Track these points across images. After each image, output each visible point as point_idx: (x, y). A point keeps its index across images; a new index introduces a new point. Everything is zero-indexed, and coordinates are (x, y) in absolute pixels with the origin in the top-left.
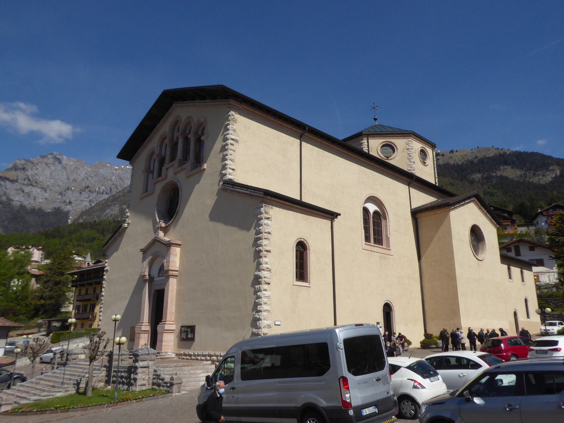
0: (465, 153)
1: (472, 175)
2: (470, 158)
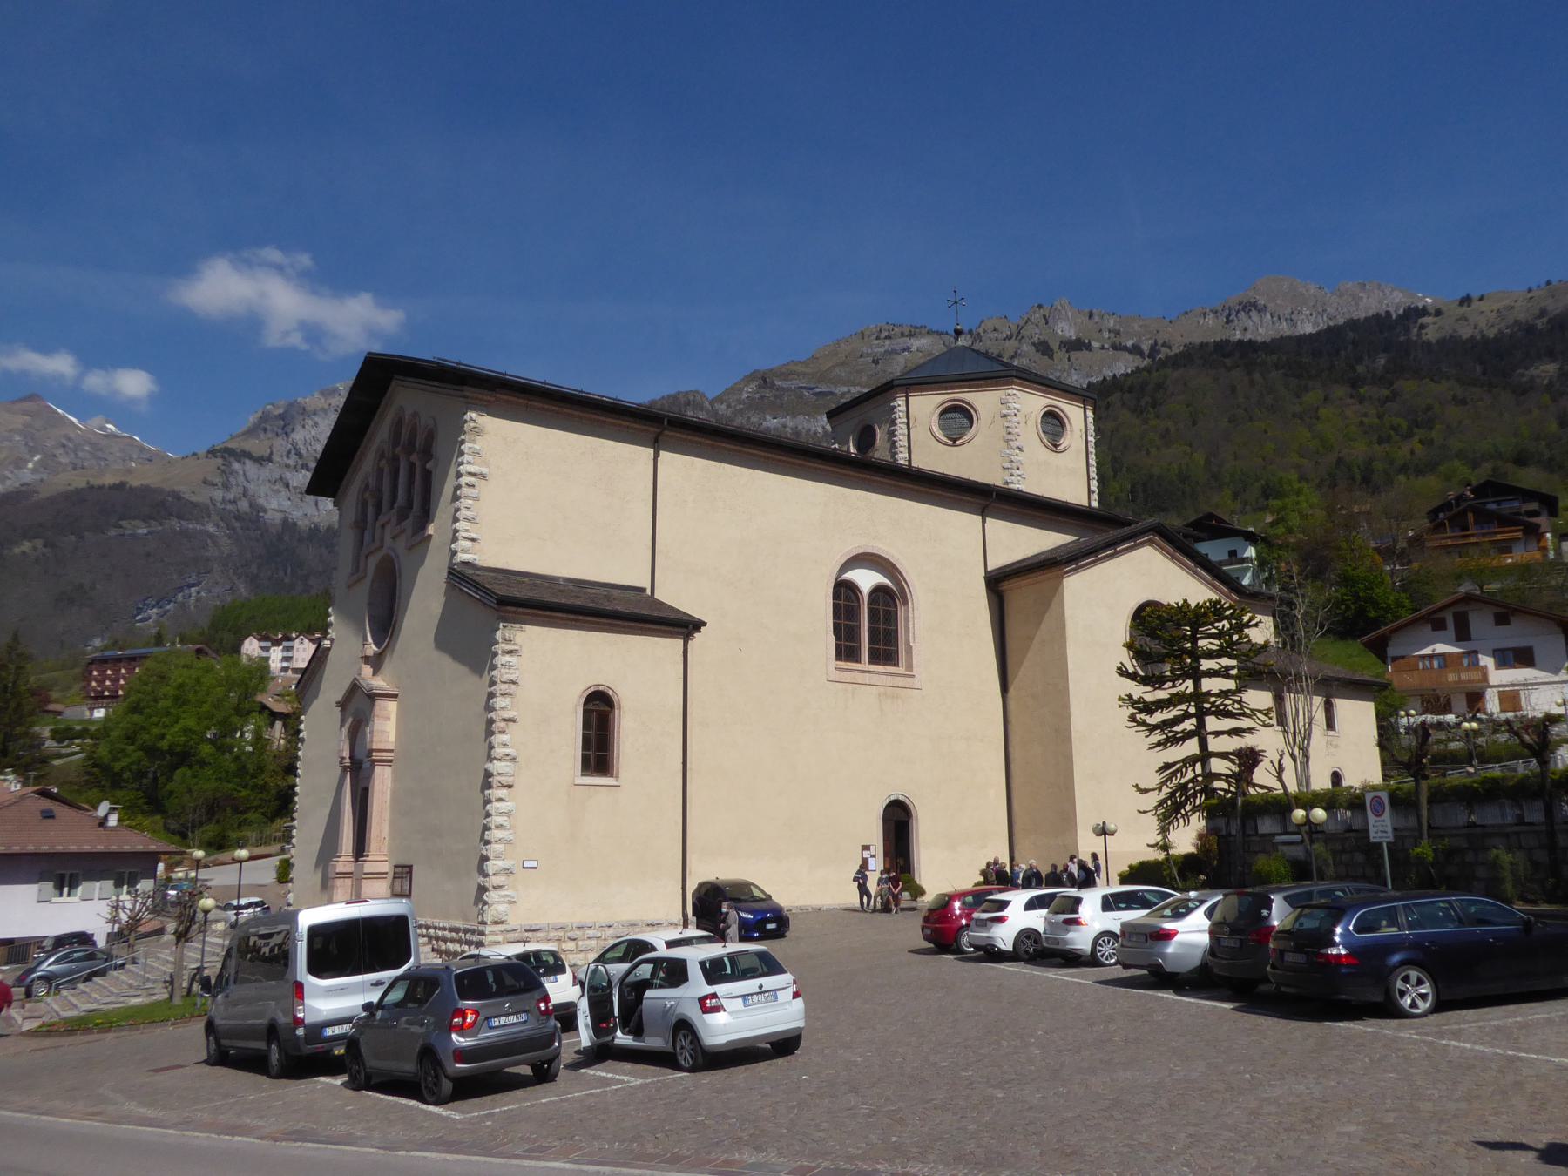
0: (1506, 302)
1: (1527, 369)
2: (1522, 317)
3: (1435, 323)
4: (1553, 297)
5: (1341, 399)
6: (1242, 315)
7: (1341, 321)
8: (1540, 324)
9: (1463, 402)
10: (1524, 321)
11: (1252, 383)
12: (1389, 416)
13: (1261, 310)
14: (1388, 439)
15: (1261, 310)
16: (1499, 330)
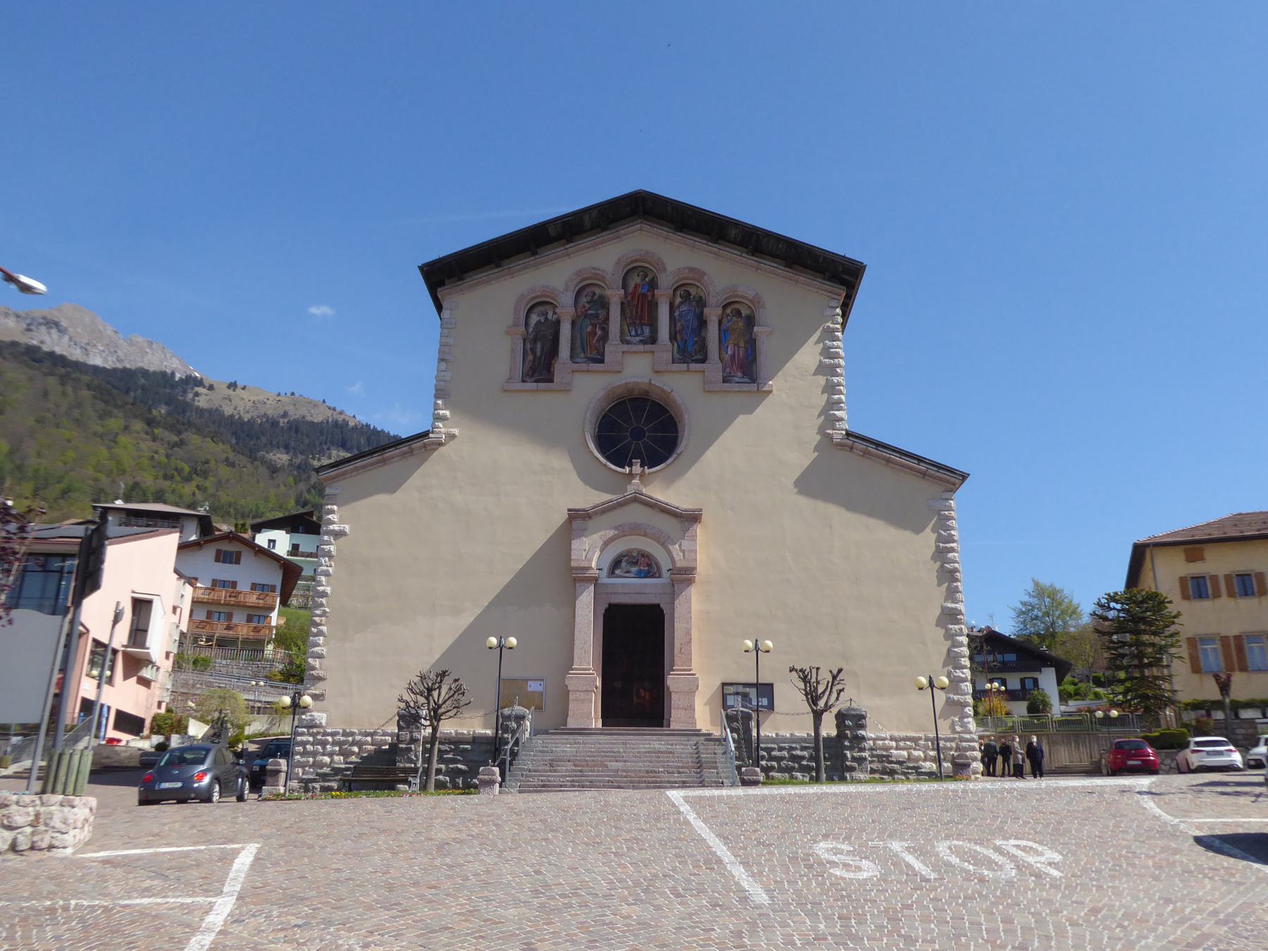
0: (261, 398)
1: (268, 452)
2: (270, 413)
3: (206, 395)
4: (295, 405)
5: (138, 433)
6: (43, 329)
7: (45, 348)
8: (282, 422)
9: (232, 465)
10: (270, 416)
11: (64, 394)
12: (176, 459)
13: (62, 331)
14: (171, 478)
15: (62, 331)
16: (252, 417)
